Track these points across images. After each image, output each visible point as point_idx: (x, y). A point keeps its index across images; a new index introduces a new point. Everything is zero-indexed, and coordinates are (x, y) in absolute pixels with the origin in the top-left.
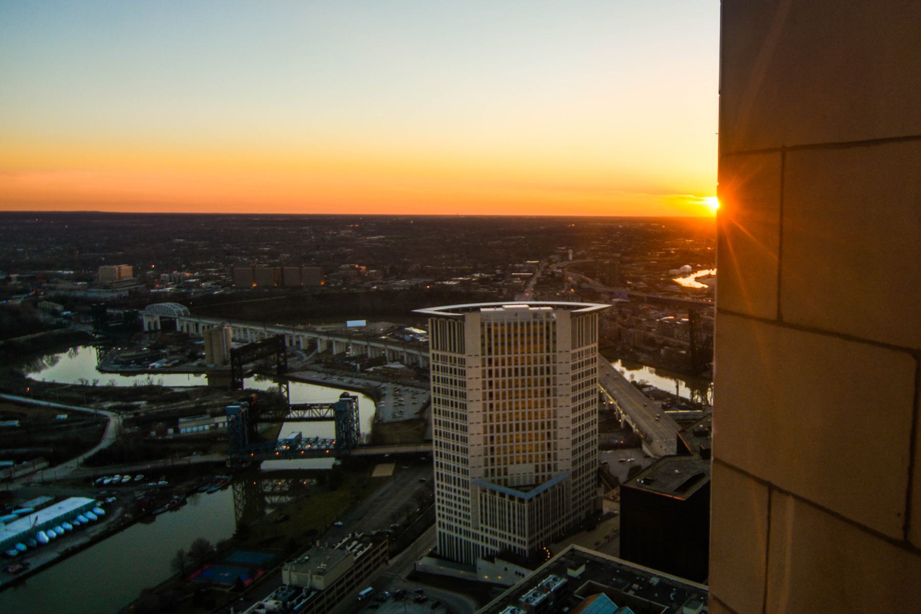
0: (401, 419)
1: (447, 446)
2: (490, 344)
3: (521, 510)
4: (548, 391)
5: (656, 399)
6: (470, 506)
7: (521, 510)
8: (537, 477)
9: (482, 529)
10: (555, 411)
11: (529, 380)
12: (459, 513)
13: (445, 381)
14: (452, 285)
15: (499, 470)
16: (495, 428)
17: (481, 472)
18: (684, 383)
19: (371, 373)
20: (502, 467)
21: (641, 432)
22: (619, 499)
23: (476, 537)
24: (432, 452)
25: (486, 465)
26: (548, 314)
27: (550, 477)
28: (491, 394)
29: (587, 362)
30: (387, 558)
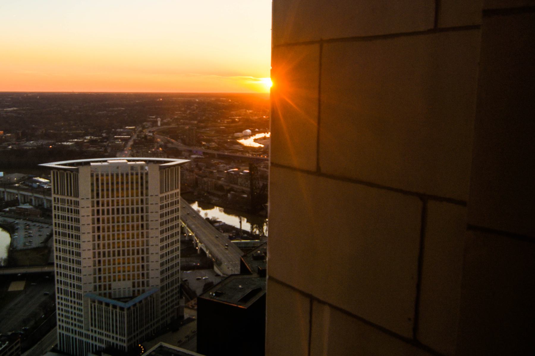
0: (30, 247)
1: (65, 268)
2: (98, 190)
3: (122, 316)
4: (142, 225)
5: (224, 232)
6: (83, 313)
7: (122, 316)
8: (134, 291)
9: (92, 331)
10: (147, 241)
11: (128, 217)
12: (73, 317)
13: (63, 218)
14: (68, 146)
15: (105, 285)
16: (102, 254)
17: (91, 287)
18: (246, 219)
19: (8, 212)
20: (107, 283)
21: (213, 256)
22: (196, 307)
23: (87, 336)
24: (54, 272)
25: (95, 282)
26: (142, 167)
27: (144, 291)
28: (99, 228)
29: (172, 204)
30: (20, 353)
